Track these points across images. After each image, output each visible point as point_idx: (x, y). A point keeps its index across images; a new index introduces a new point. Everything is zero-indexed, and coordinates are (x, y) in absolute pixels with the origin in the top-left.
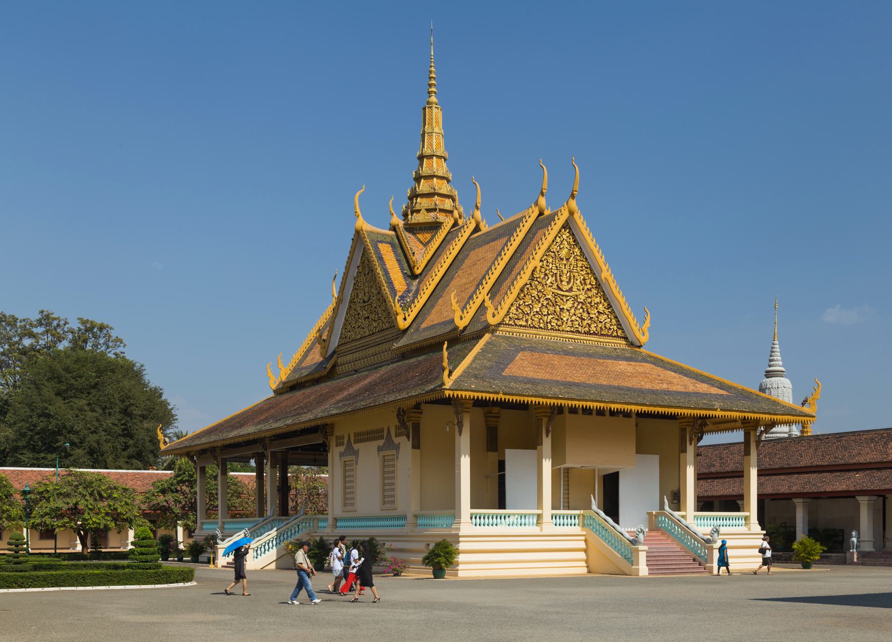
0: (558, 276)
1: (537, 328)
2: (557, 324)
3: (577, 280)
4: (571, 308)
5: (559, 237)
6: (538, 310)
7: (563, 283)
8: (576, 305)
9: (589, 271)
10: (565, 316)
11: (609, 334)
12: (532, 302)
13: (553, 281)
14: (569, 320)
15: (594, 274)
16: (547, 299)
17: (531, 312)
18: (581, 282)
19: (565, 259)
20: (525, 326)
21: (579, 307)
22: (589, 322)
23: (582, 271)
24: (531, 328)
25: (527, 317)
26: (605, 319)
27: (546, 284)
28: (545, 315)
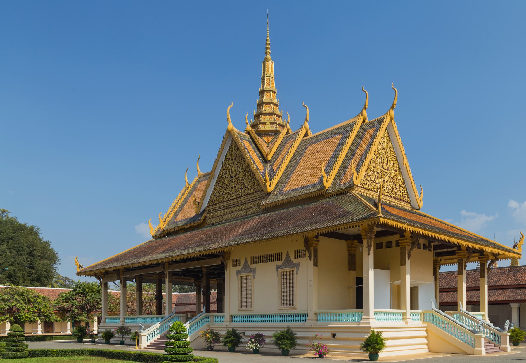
3: (239, 168)
4: (236, 185)
7: (233, 172)
11: (254, 192)
16: (227, 185)
21: (240, 183)
24: (220, 203)
27: (226, 178)
28: (225, 194)
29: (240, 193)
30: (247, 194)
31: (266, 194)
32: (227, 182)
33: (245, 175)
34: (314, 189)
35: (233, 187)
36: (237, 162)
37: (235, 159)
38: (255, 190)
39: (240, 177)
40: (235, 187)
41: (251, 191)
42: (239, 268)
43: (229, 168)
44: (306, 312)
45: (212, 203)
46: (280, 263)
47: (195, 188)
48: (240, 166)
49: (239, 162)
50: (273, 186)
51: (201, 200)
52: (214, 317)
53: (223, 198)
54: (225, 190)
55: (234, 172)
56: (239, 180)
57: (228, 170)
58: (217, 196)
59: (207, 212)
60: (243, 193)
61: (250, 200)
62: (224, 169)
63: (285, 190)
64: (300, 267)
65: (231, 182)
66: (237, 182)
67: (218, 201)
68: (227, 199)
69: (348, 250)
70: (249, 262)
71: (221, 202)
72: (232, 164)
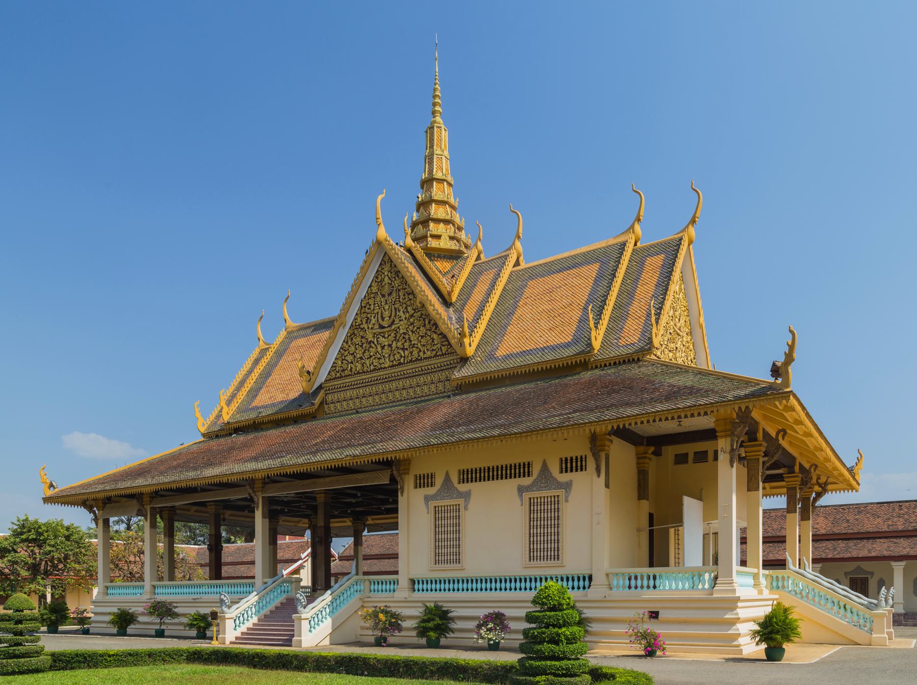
1: (362, 373)
3: (399, 311)
4: (392, 342)
6: (362, 355)
7: (385, 319)
8: (397, 338)
11: (433, 355)
16: (371, 341)
21: (401, 338)
24: (355, 374)
27: (368, 328)
28: (368, 358)
29: (401, 357)
30: (417, 360)
31: (459, 360)
32: (371, 336)
33: (411, 324)
34: (567, 353)
35: (385, 346)
36: (394, 300)
37: (390, 294)
38: (434, 352)
39: (401, 327)
40: (390, 345)
41: (424, 353)
42: (431, 491)
43: (376, 311)
44: (589, 572)
46: (526, 481)
47: (285, 350)
48: (401, 307)
49: (399, 301)
50: (474, 345)
51: (315, 368)
52: (371, 582)
53: (363, 365)
54: (367, 351)
55: (388, 318)
56: (397, 332)
57: (373, 315)
58: (350, 361)
59: (326, 390)
60: (408, 357)
61: (422, 370)
62: (363, 313)
63: (500, 353)
64: (573, 488)
65: (381, 337)
66: (395, 337)
67: (351, 370)
68: (372, 367)
69: (637, 464)
70: (454, 479)
71: (358, 373)
72: (382, 304)
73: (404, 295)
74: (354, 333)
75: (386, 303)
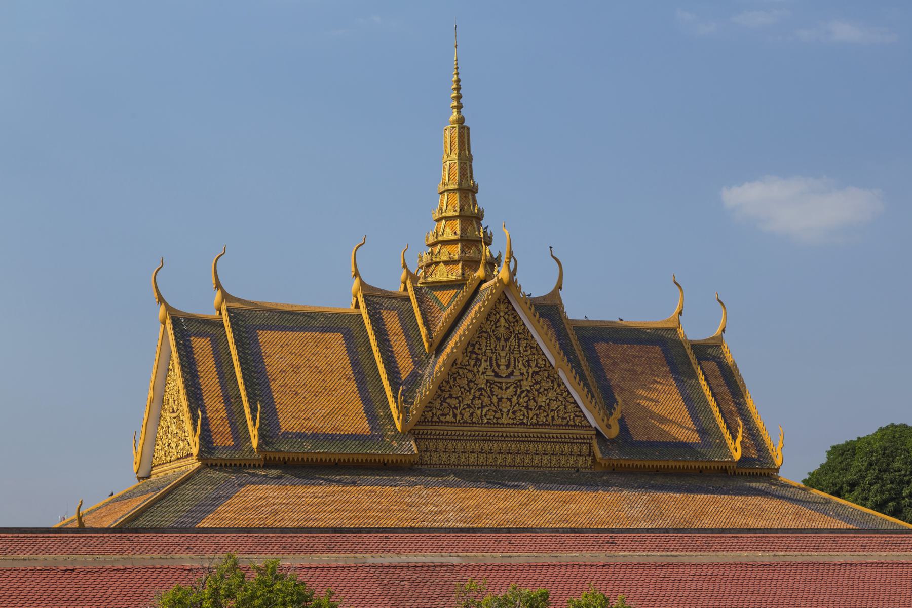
0: (494, 359)
2: (494, 417)
3: (519, 362)
4: (512, 396)
5: (495, 315)
6: (469, 402)
7: (501, 367)
8: (518, 392)
9: (534, 351)
10: (505, 406)
11: (564, 423)
12: (462, 393)
13: (487, 366)
14: (511, 411)
15: (543, 354)
16: (480, 389)
17: (460, 406)
18: (523, 364)
19: (502, 339)
20: (455, 423)
22: (537, 412)
23: (526, 351)
25: (455, 411)
26: (559, 406)
27: (478, 372)
28: (478, 408)
30: (544, 424)
35: (502, 398)
45: (435, 419)
48: (522, 359)
49: (520, 351)
60: (532, 419)
66: (517, 390)
73: (526, 347)
74: (458, 373)
75: (503, 350)
